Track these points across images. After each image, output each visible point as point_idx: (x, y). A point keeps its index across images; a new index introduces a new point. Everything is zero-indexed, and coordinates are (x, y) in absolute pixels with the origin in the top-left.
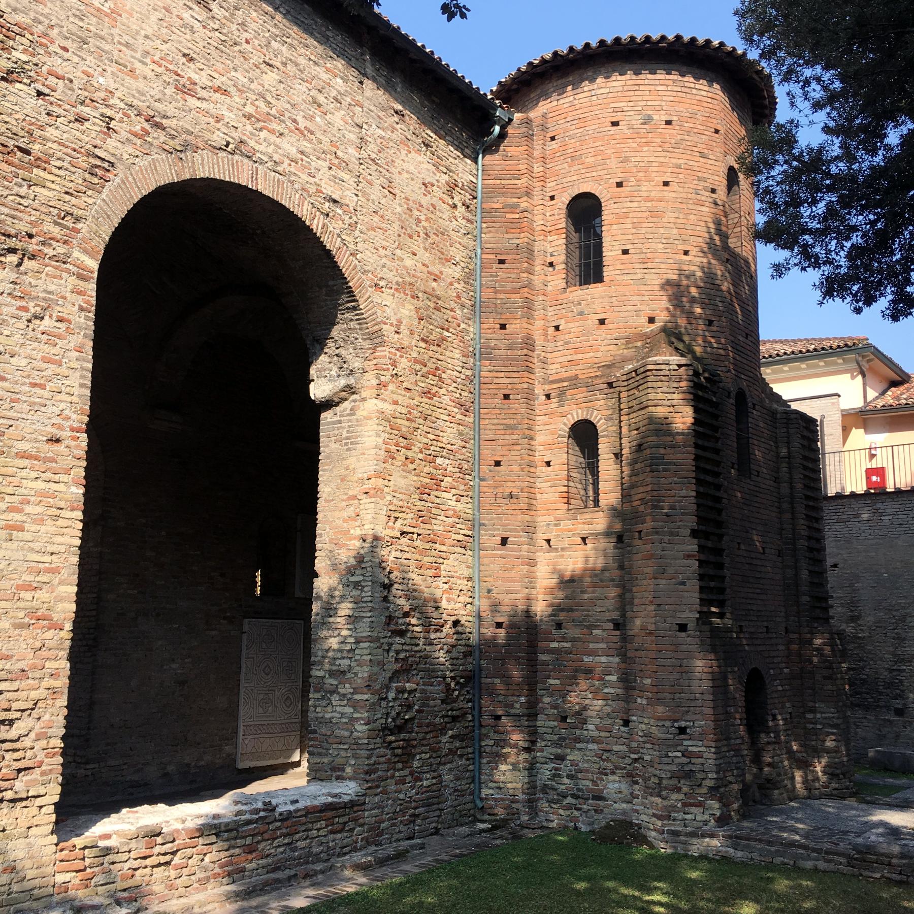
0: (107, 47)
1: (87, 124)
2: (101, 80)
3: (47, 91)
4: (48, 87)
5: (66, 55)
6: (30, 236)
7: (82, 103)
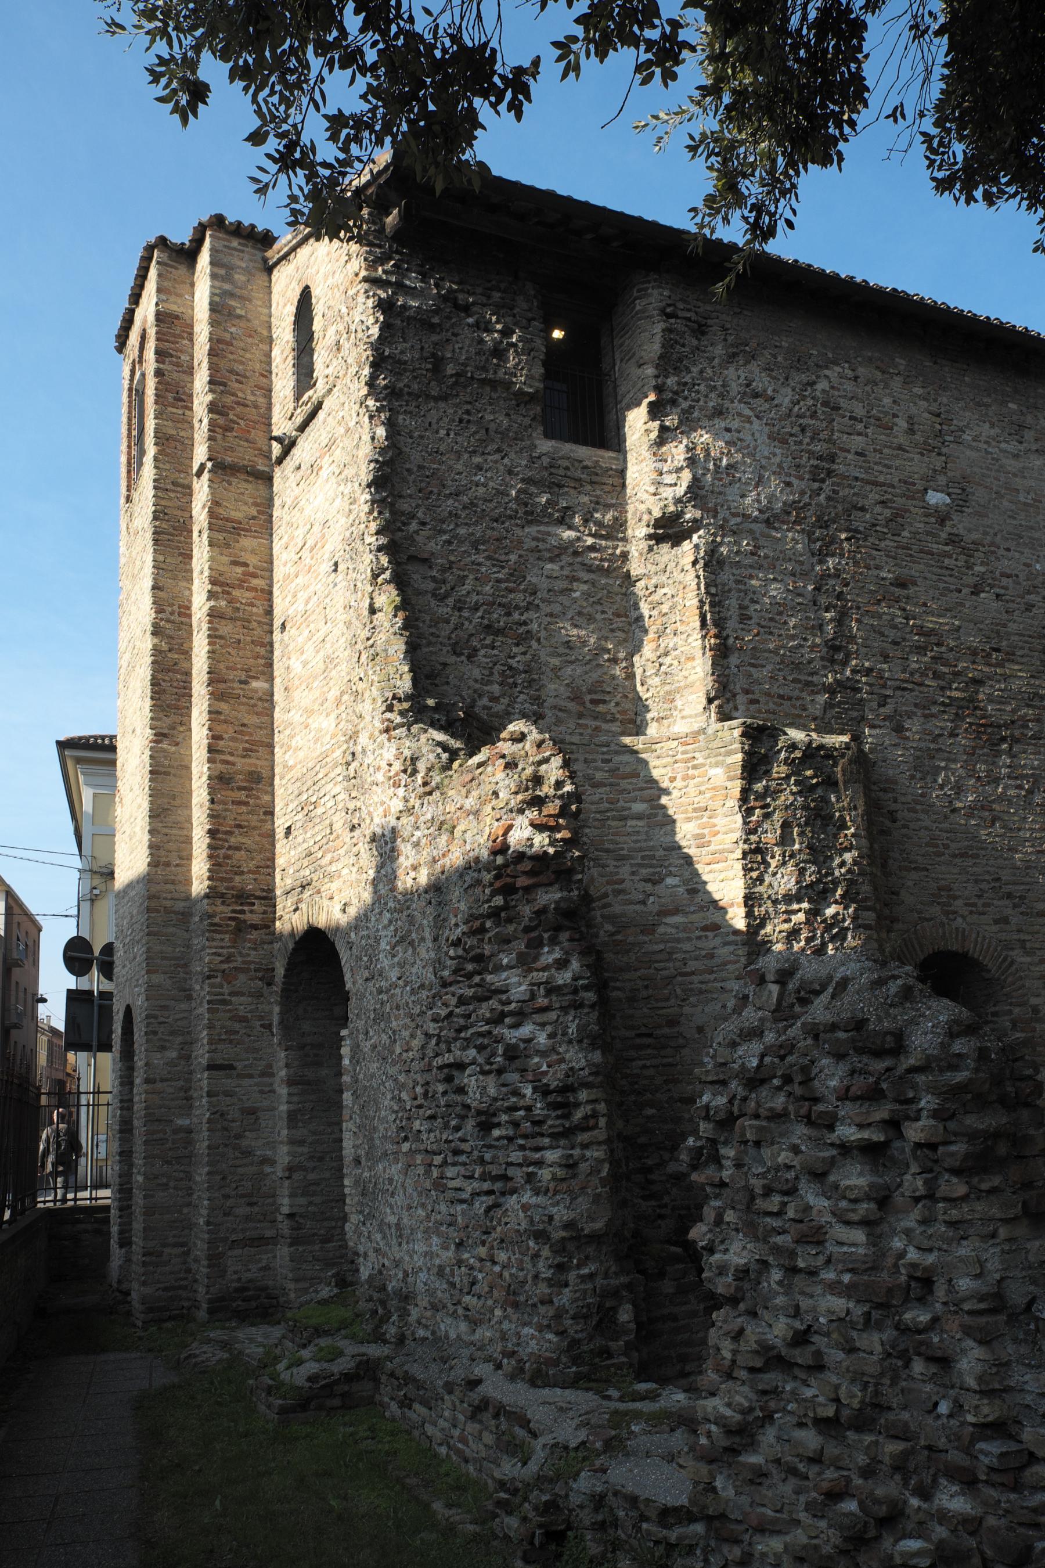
0: (1037, 535)
1: (1035, 611)
2: (1038, 567)
3: (1002, 591)
4: (1002, 587)
5: (1010, 554)
6: (1013, 722)
7: (1029, 593)
